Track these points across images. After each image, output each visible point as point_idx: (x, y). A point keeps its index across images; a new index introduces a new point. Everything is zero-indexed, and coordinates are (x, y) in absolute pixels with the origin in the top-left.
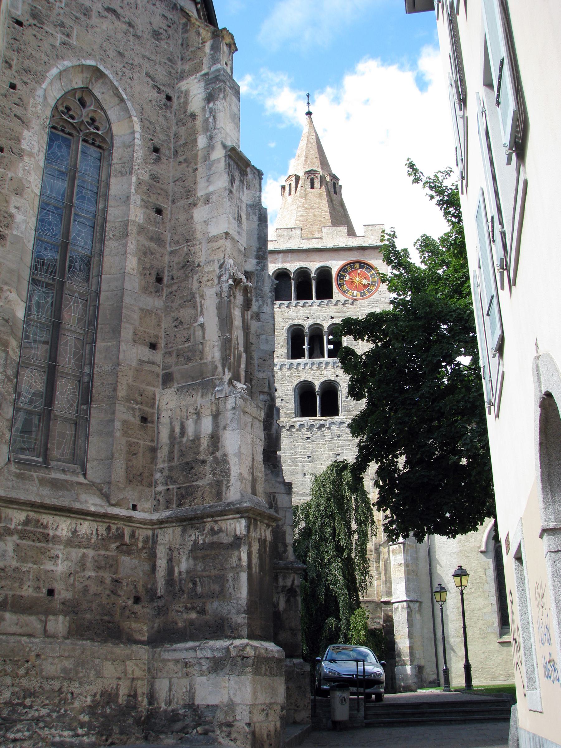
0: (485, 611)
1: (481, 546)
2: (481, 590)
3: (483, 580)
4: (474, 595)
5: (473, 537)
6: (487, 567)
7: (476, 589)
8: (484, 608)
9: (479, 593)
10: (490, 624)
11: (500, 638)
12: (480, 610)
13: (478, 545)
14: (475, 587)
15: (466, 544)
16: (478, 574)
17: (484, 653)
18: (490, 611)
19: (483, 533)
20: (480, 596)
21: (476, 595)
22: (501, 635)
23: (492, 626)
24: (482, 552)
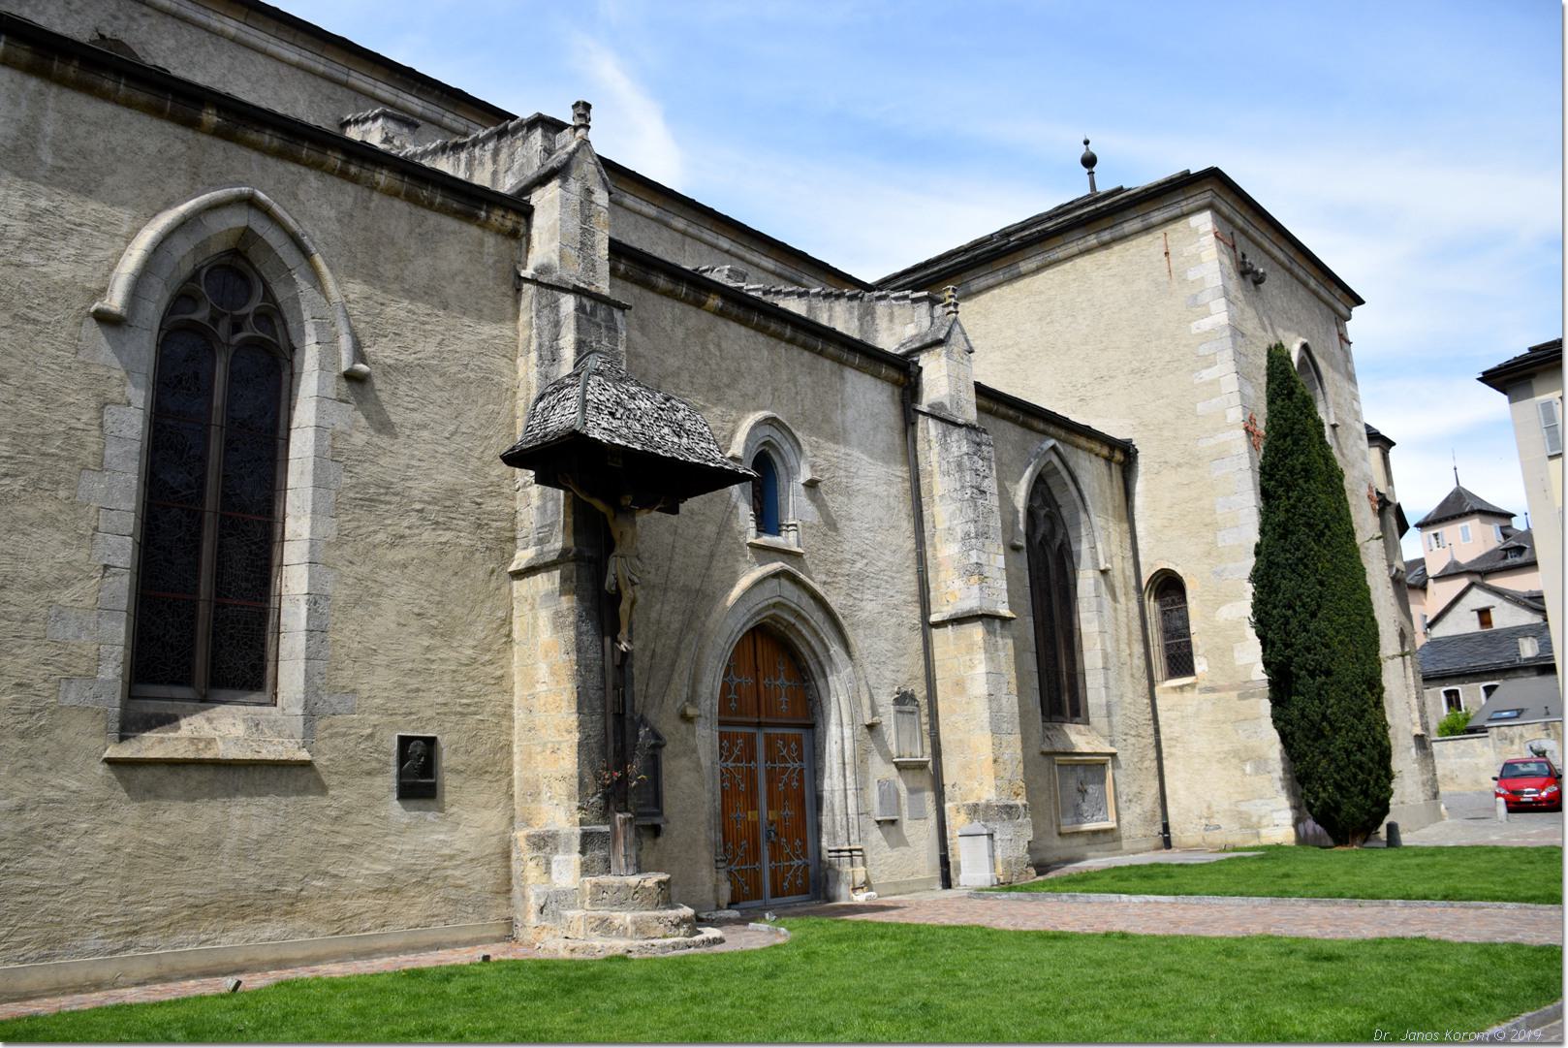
0: (65, 597)
1: (102, 292)
2: (62, 494)
3: (82, 445)
4: (20, 510)
5: (75, 240)
6: (114, 394)
7: (36, 484)
8: (63, 582)
9: (50, 507)
10: (82, 666)
11: (122, 739)
12: (37, 588)
13: (93, 285)
14: (34, 475)
15: (30, 258)
16: (59, 415)
17: (20, 809)
18: (89, 601)
19: (129, 239)
20: (52, 522)
21: (31, 512)
22: (130, 726)
23: (90, 676)
24: (104, 319)
